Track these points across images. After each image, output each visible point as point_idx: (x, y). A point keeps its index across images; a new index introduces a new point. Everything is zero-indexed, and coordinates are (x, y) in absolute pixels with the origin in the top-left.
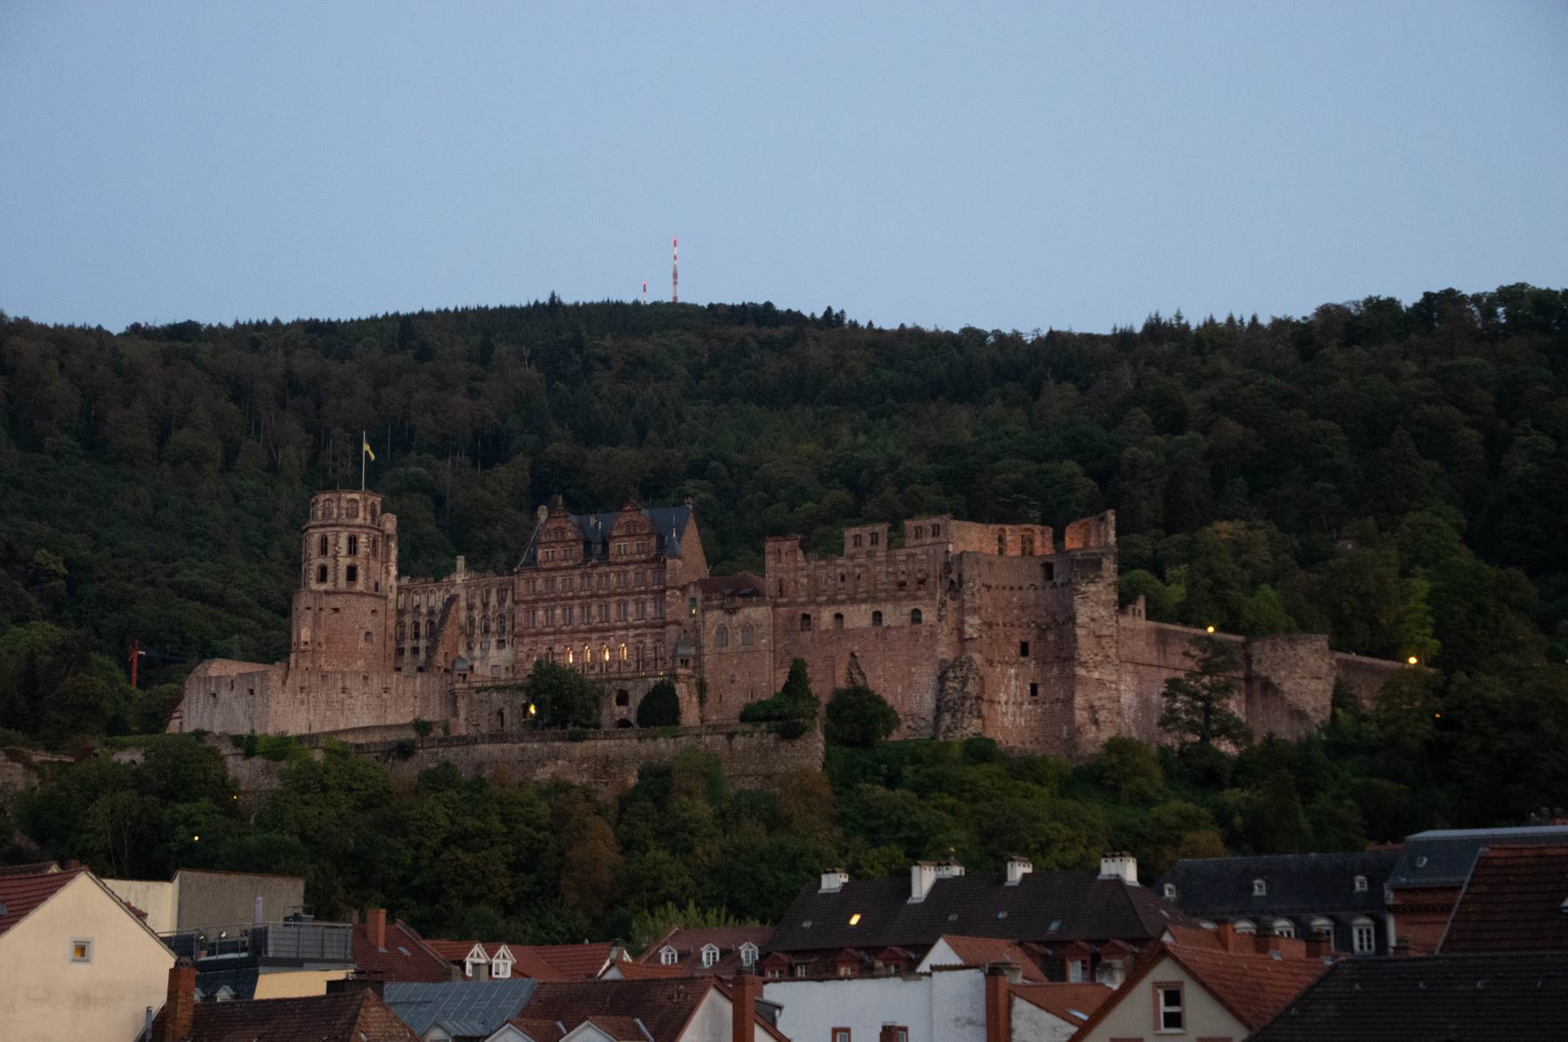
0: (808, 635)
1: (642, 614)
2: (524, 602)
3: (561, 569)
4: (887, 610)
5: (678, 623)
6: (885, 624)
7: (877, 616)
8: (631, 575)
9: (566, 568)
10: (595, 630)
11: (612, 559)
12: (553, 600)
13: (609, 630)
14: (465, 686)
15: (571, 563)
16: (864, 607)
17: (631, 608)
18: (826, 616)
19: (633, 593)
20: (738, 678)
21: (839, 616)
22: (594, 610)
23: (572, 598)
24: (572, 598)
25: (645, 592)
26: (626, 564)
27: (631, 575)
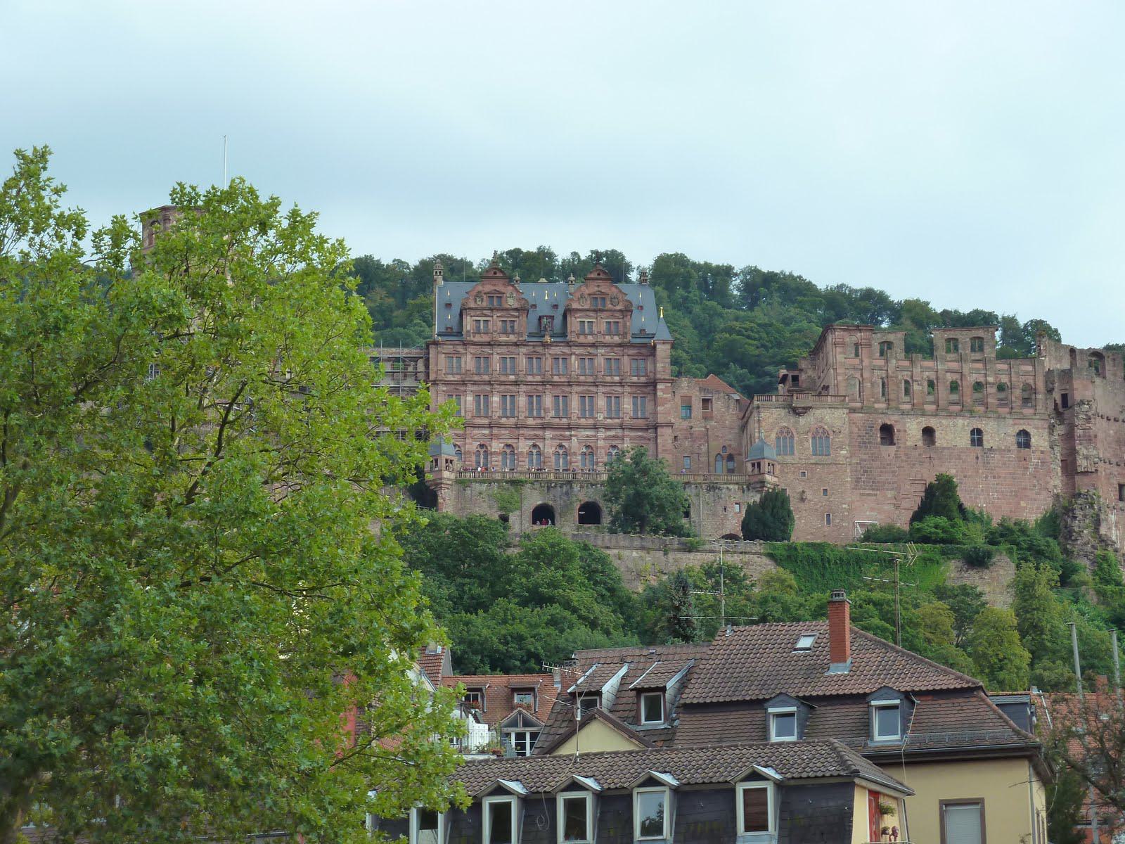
0: (894, 448)
2: (447, 383)
3: (500, 344)
4: (988, 427)
5: (670, 425)
6: (986, 445)
7: (977, 436)
8: (600, 362)
9: (507, 344)
13: (569, 428)
15: (512, 338)
16: (960, 421)
17: (601, 402)
18: (911, 429)
19: (604, 384)
20: (809, 495)
21: (928, 432)
22: (548, 401)
24: (516, 383)
25: (621, 384)
27: (600, 362)
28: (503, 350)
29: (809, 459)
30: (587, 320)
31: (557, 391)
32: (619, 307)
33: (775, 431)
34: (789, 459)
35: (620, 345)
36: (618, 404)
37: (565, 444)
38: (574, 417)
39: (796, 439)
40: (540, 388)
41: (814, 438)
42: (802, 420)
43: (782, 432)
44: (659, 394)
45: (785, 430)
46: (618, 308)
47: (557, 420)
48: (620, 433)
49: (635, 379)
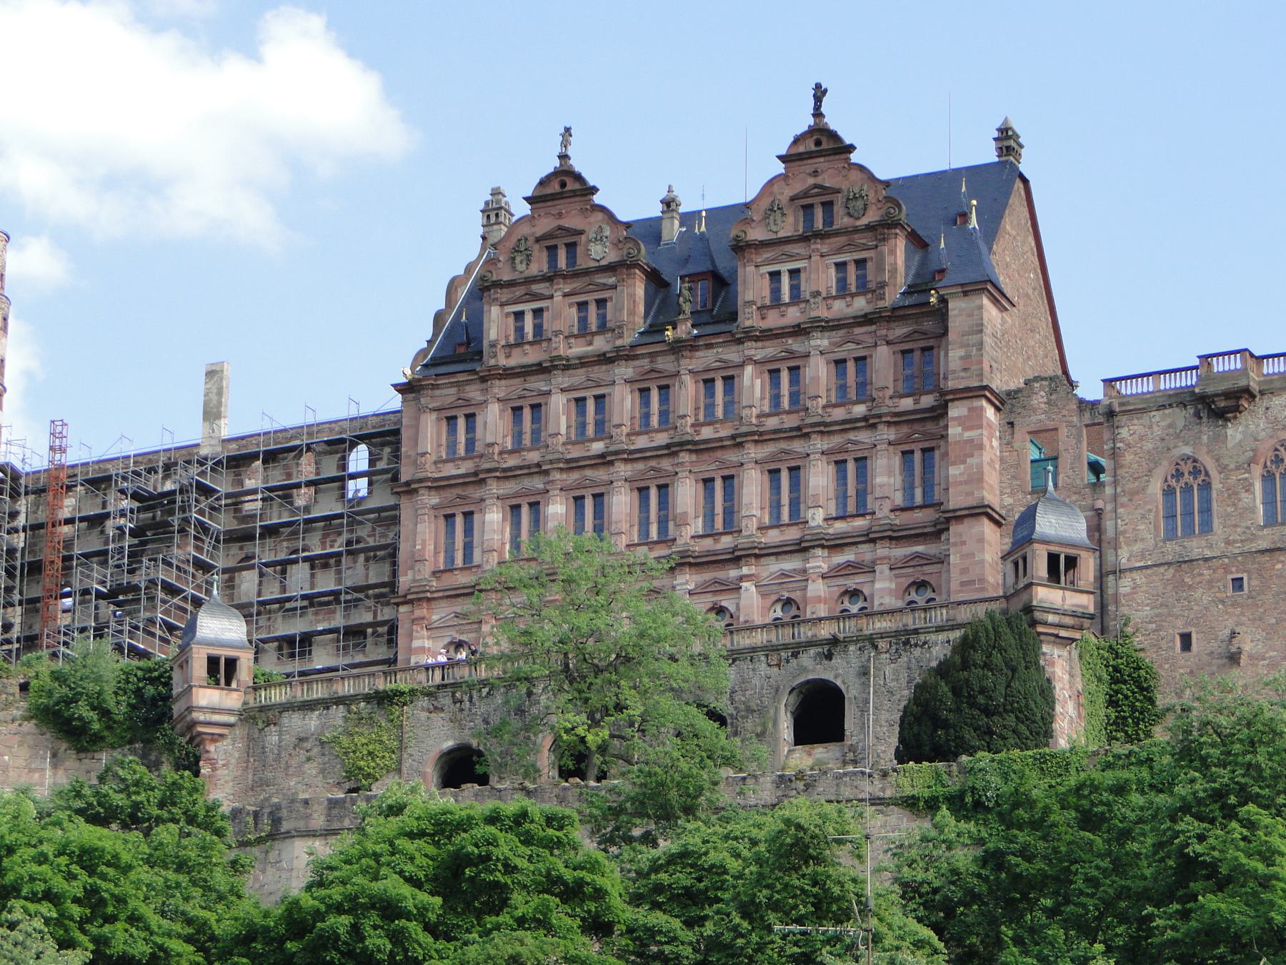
1: (855, 499)
8: (819, 372)
10: (687, 562)
11: (749, 319)
12: (538, 470)
13: (735, 558)
14: (231, 699)
15: (600, 344)
17: (820, 478)
19: (824, 429)
22: (686, 494)
23: (604, 460)
24: (604, 460)
25: (869, 422)
26: (799, 331)
27: (819, 372)
28: (578, 377)
29: (1254, 538)
30: (784, 268)
31: (708, 466)
32: (872, 216)
33: (1164, 468)
34: (1196, 547)
35: (866, 319)
36: (862, 475)
37: (727, 602)
38: (750, 527)
39: (1216, 485)
40: (666, 464)
41: (1268, 478)
42: (1234, 432)
43: (1178, 475)
44: (954, 431)
45: (1186, 468)
46: (864, 221)
47: (708, 544)
48: (865, 553)
49: (907, 404)
